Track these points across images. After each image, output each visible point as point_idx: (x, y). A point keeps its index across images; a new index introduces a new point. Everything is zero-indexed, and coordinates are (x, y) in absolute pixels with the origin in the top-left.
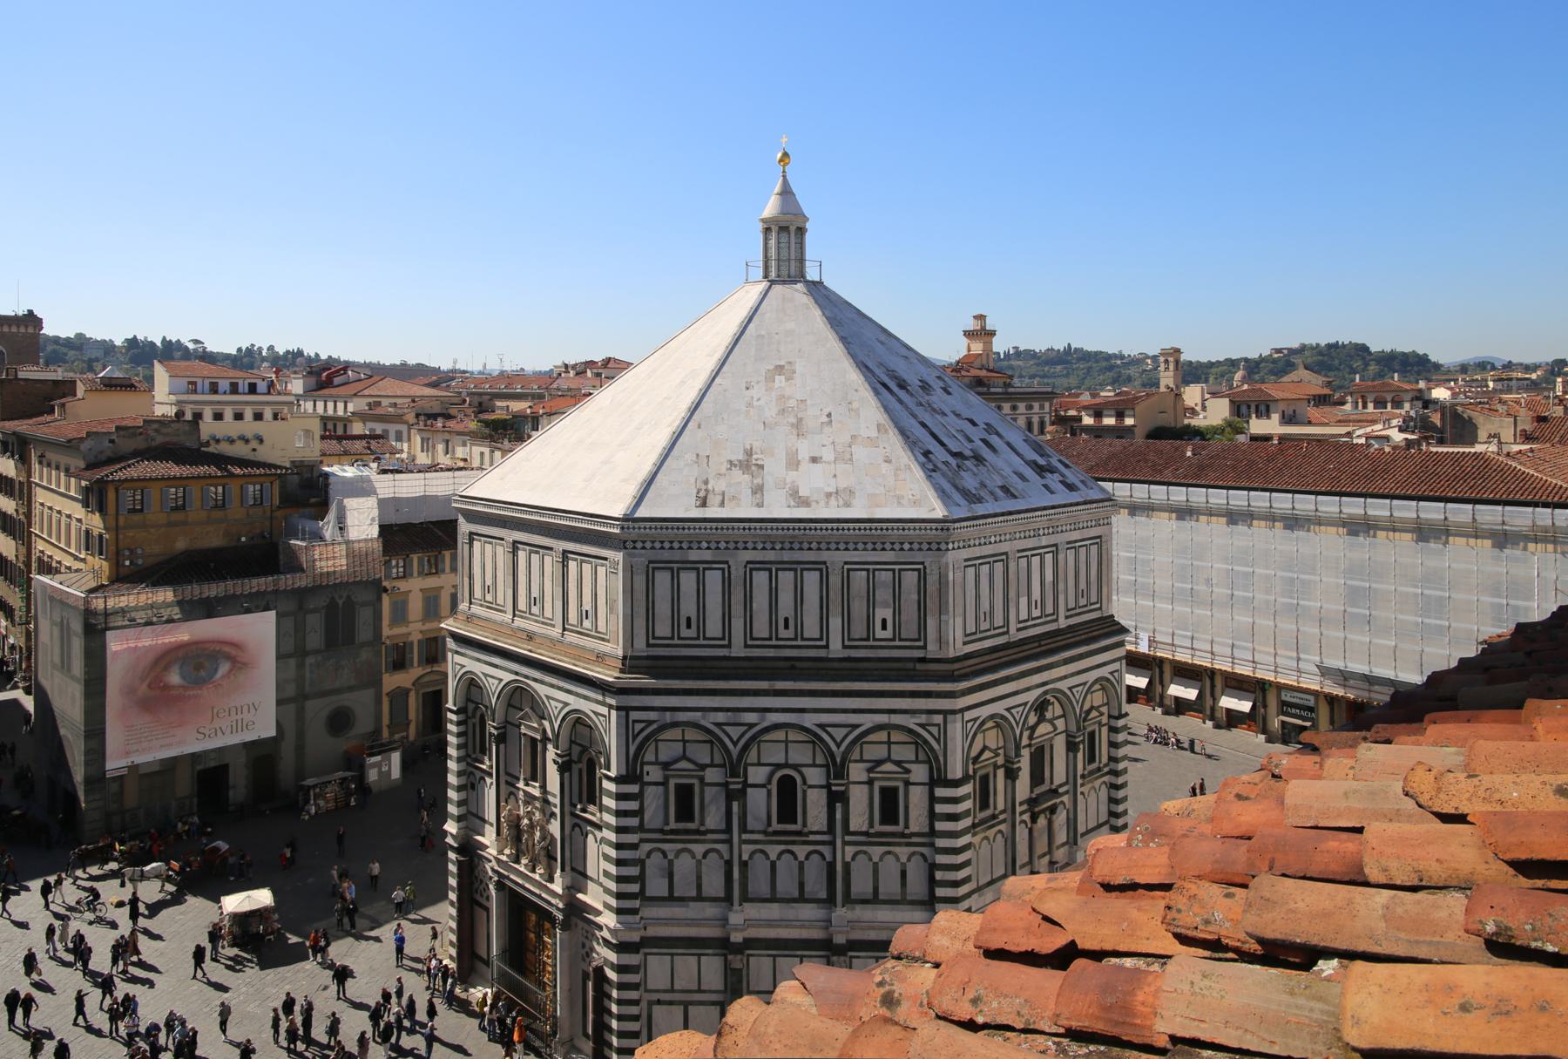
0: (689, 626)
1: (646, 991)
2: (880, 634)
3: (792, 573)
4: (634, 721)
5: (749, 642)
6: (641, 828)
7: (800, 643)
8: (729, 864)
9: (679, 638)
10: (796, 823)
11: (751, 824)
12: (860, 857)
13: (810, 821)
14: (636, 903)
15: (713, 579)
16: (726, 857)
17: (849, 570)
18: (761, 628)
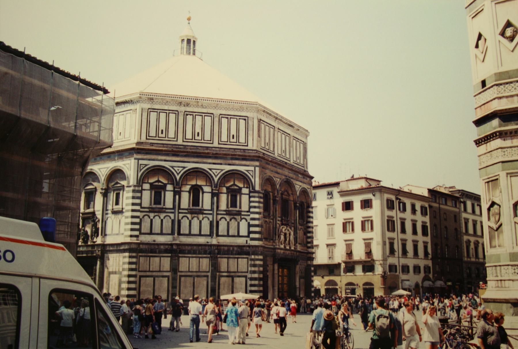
0: (162, 133)
1: (139, 271)
2: (232, 140)
3: (201, 117)
4: (141, 165)
5: (184, 140)
6: (140, 204)
7: (203, 141)
8: (173, 221)
9: (158, 137)
10: (199, 206)
11: (182, 207)
12: (223, 220)
13: (204, 206)
14: (137, 233)
15: (172, 117)
16: (173, 218)
17: (222, 117)
18: (189, 136)
